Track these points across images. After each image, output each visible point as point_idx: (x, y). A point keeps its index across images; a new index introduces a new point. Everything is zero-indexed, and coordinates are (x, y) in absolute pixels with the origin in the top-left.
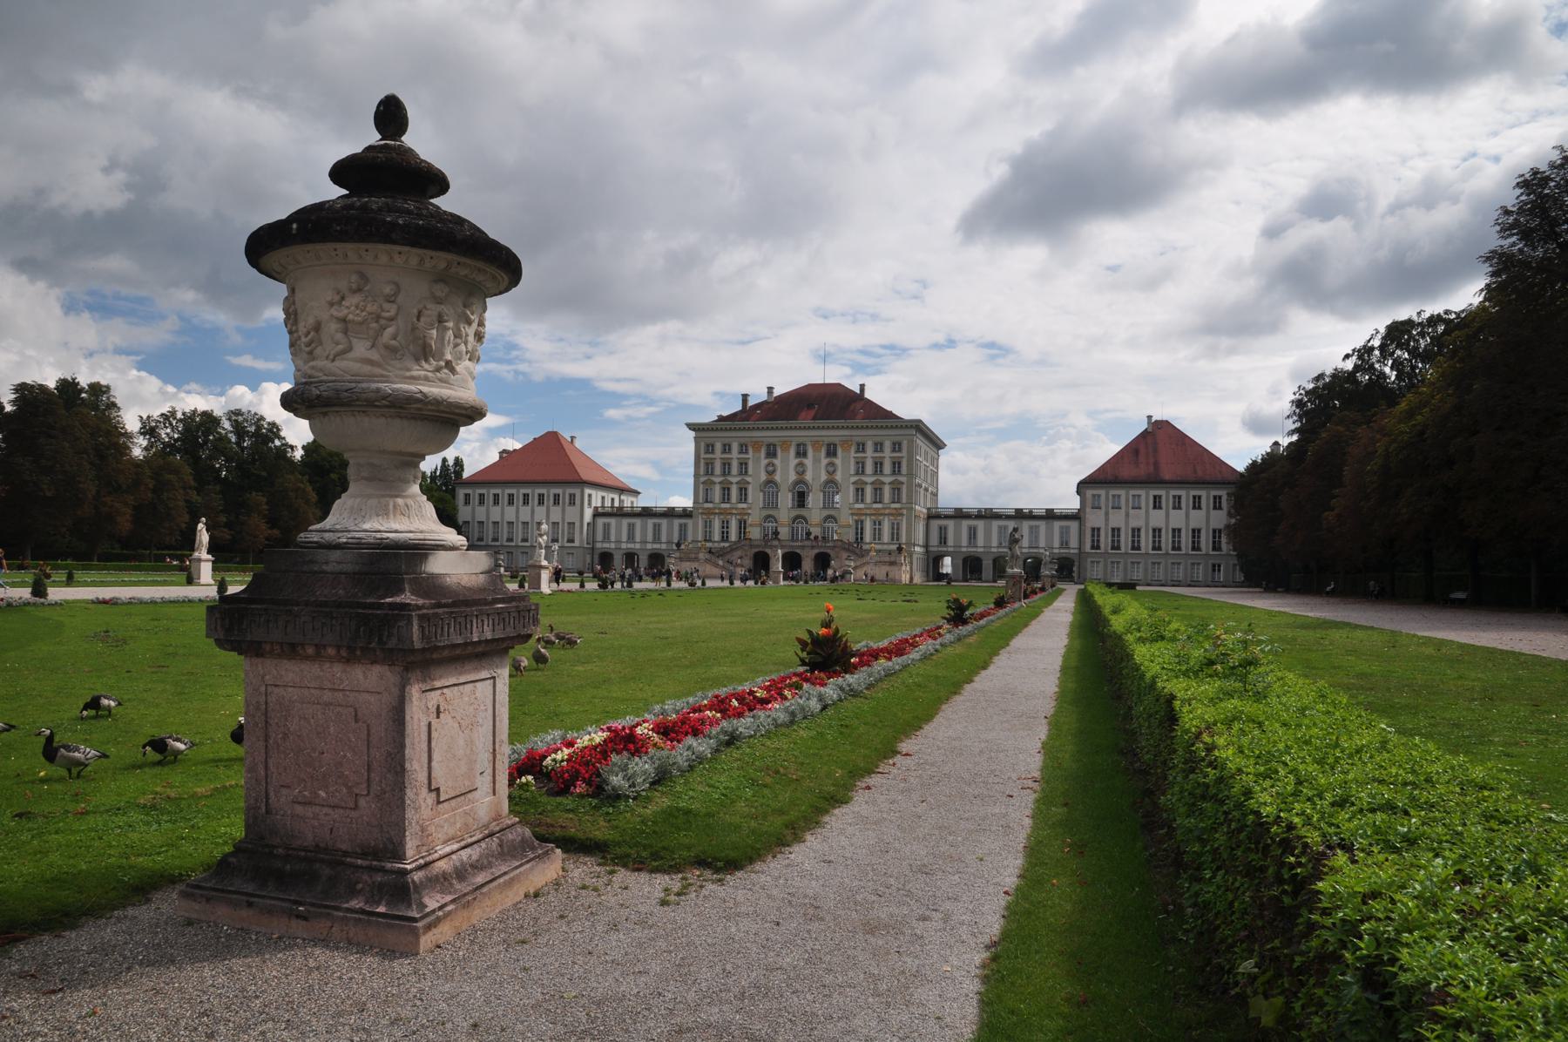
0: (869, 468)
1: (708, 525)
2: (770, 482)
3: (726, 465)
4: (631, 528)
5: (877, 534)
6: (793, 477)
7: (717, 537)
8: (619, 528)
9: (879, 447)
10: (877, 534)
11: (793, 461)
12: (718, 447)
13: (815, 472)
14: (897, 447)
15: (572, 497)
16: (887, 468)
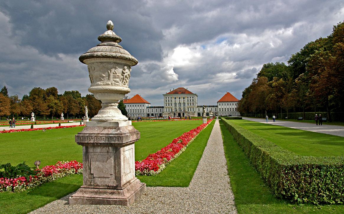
0: (189, 101)
1: (167, 109)
2: (175, 103)
3: (169, 100)
4: (152, 110)
5: (191, 110)
6: (178, 102)
7: (168, 111)
8: (150, 110)
9: (190, 98)
10: (191, 110)
11: (178, 100)
12: (167, 98)
13: (182, 101)
14: (193, 98)
15: (143, 105)
16: (192, 101)
